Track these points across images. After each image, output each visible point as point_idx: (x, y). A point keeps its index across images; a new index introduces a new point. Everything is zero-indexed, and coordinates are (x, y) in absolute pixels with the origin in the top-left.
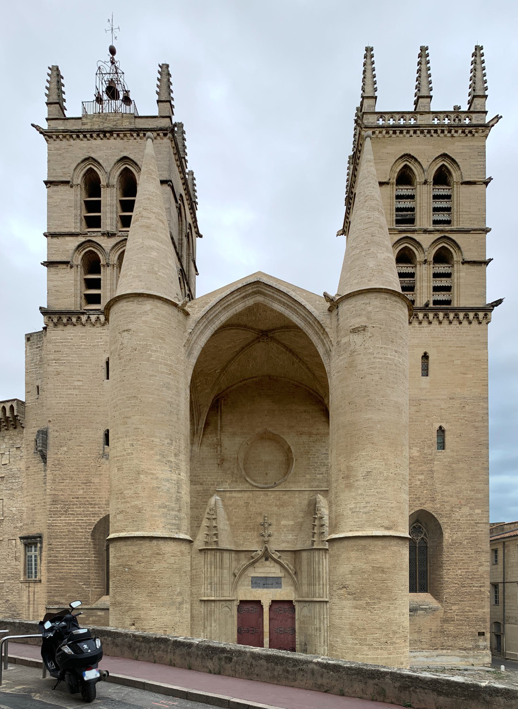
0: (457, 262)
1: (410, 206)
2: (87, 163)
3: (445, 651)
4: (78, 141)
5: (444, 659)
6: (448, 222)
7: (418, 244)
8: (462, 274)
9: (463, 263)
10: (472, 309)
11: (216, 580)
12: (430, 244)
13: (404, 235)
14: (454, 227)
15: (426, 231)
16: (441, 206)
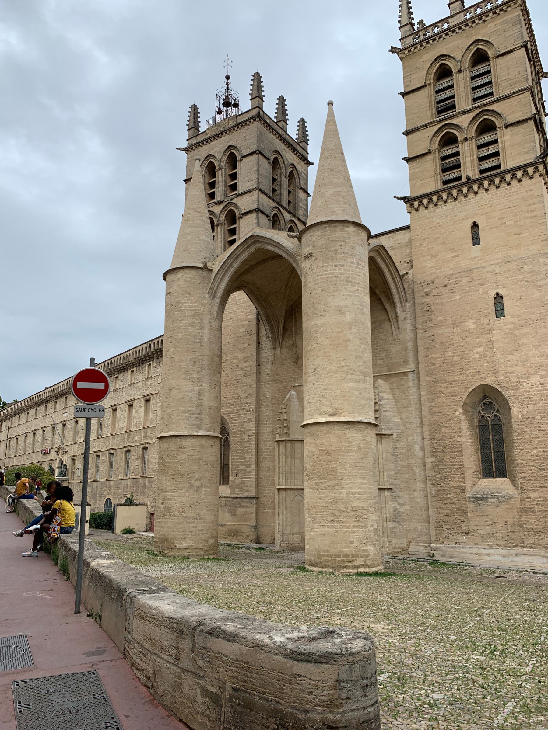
0: (500, 128)
1: (451, 95)
2: (208, 158)
3: (526, 549)
4: (204, 146)
5: (527, 559)
6: (491, 94)
7: (457, 127)
8: (507, 137)
9: (507, 127)
10: (518, 168)
11: (286, 469)
12: (469, 122)
13: (443, 123)
14: (495, 97)
15: (464, 113)
16: (482, 83)
